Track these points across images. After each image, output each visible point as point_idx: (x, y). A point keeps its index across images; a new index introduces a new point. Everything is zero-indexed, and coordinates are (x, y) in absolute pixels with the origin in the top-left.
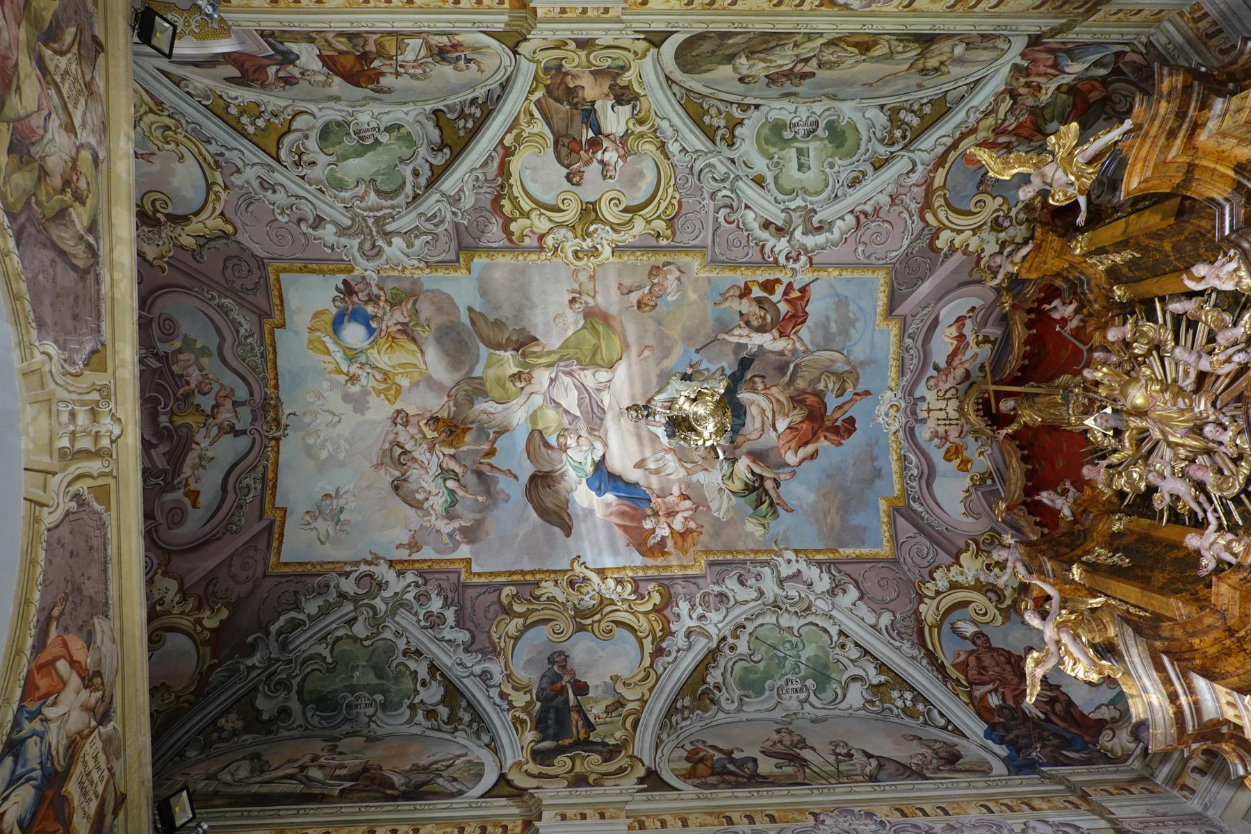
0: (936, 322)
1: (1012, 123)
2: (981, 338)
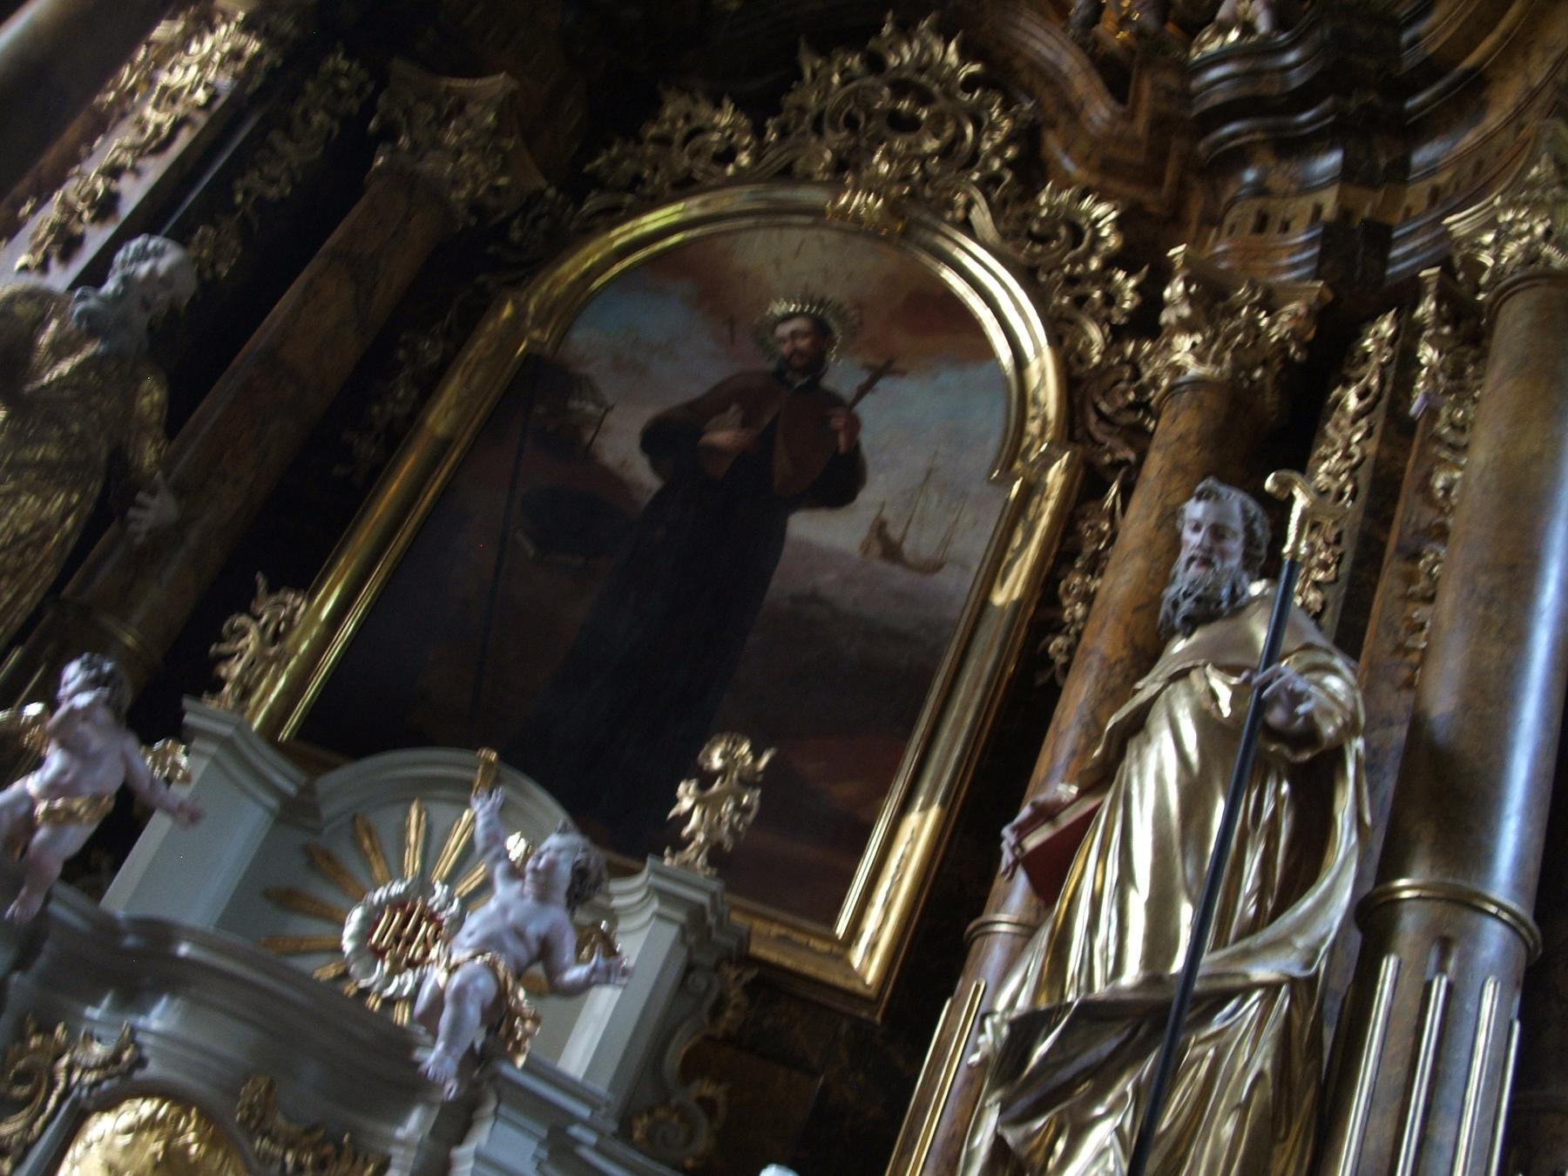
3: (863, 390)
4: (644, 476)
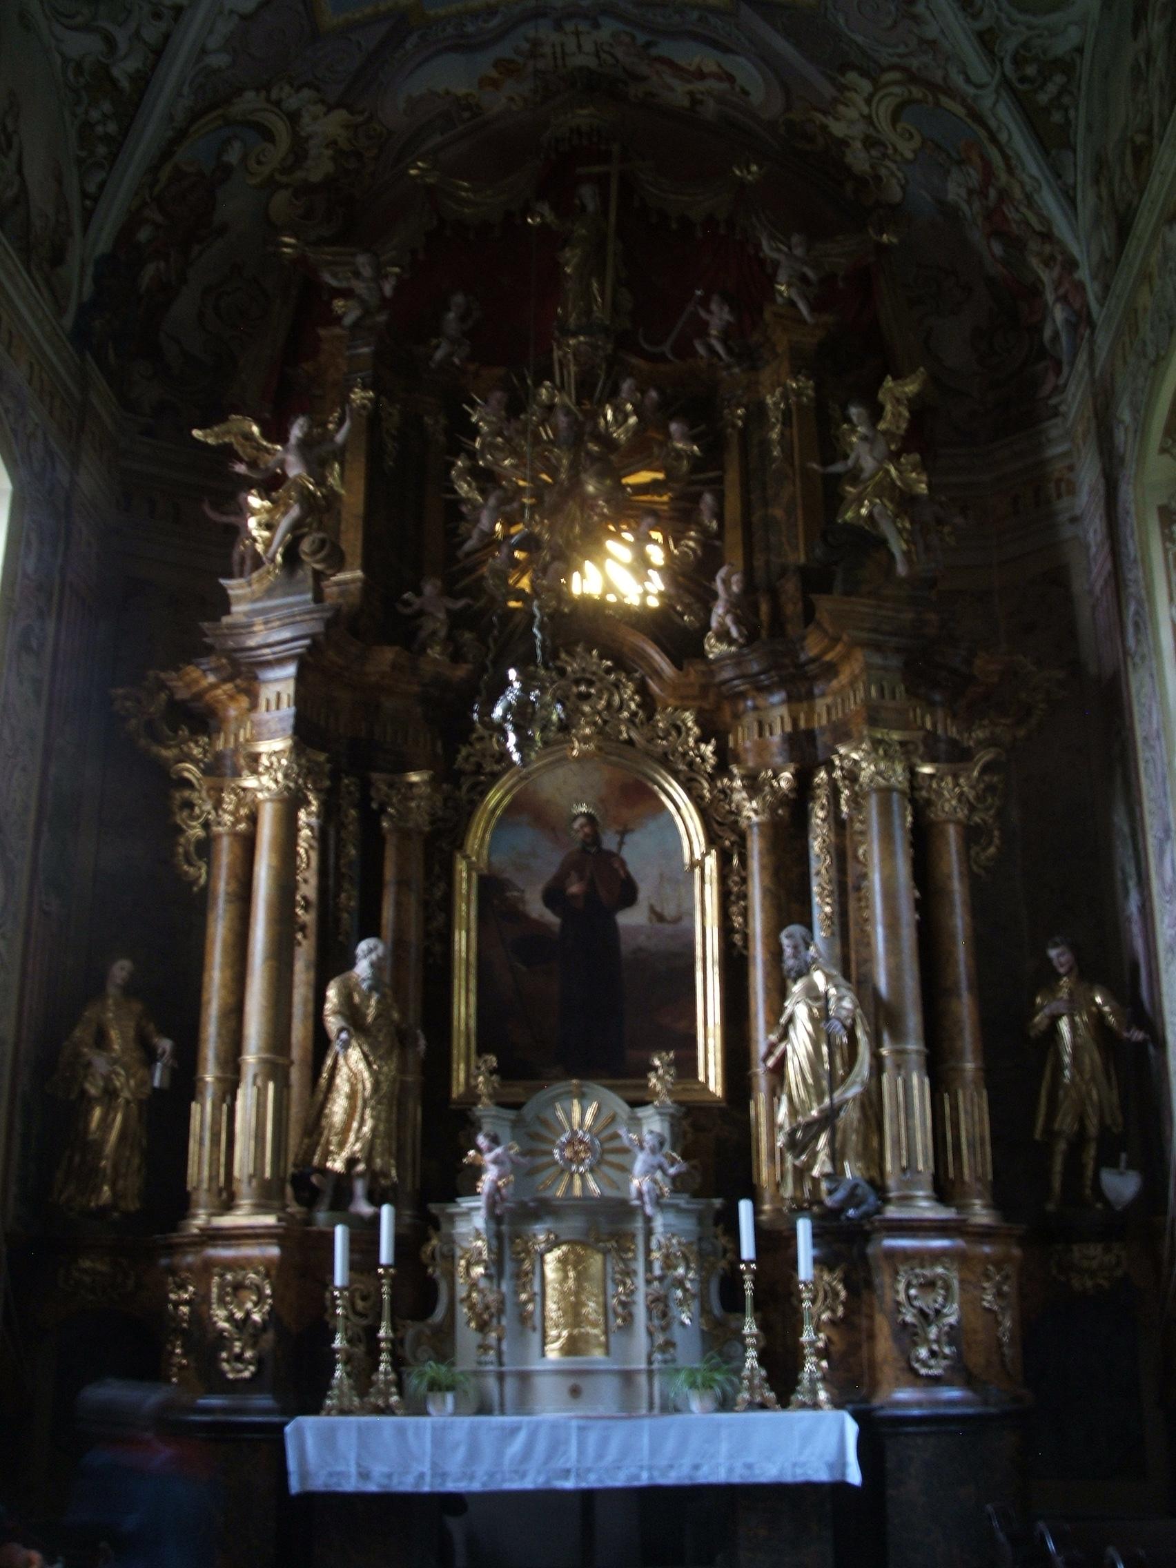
0: (727, 50)
1: (1011, 214)
2: (699, 97)
3: (621, 843)
4: (552, 919)
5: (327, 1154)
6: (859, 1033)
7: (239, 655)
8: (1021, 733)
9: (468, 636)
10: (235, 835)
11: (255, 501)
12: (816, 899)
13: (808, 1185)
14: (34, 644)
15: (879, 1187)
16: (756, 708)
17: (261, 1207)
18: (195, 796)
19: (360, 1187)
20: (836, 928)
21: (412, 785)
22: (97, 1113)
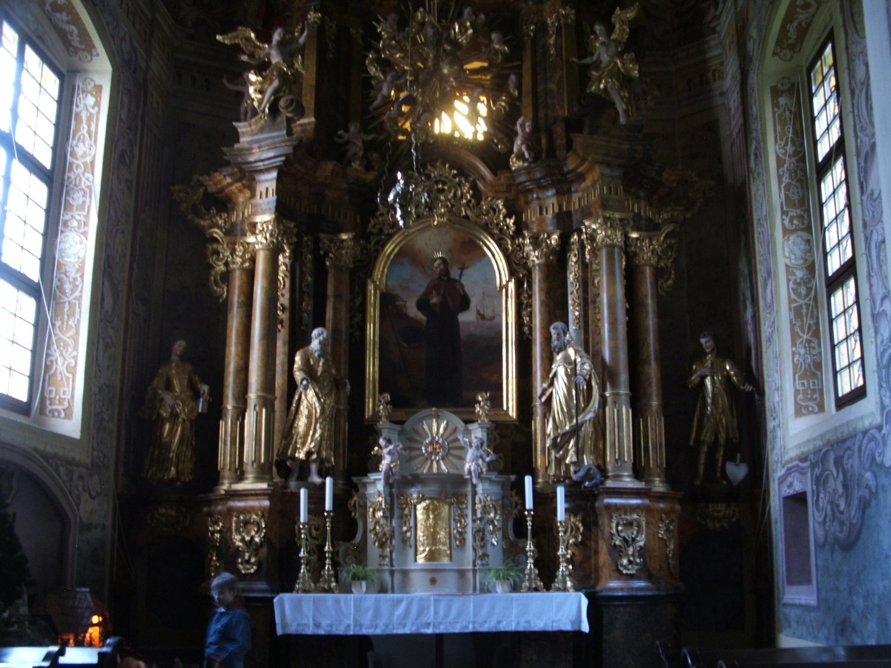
3: (461, 275)
4: (421, 317)
5: (295, 449)
6: (593, 383)
7: (244, 166)
8: (689, 215)
9: (375, 155)
10: (243, 270)
11: (253, 77)
12: (571, 308)
13: (563, 468)
14: (127, 160)
15: (602, 470)
16: (538, 198)
17: (259, 479)
18: (220, 248)
19: (314, 467)
20: (582, 324)
21: (343, 241)
22: (167, 427)
